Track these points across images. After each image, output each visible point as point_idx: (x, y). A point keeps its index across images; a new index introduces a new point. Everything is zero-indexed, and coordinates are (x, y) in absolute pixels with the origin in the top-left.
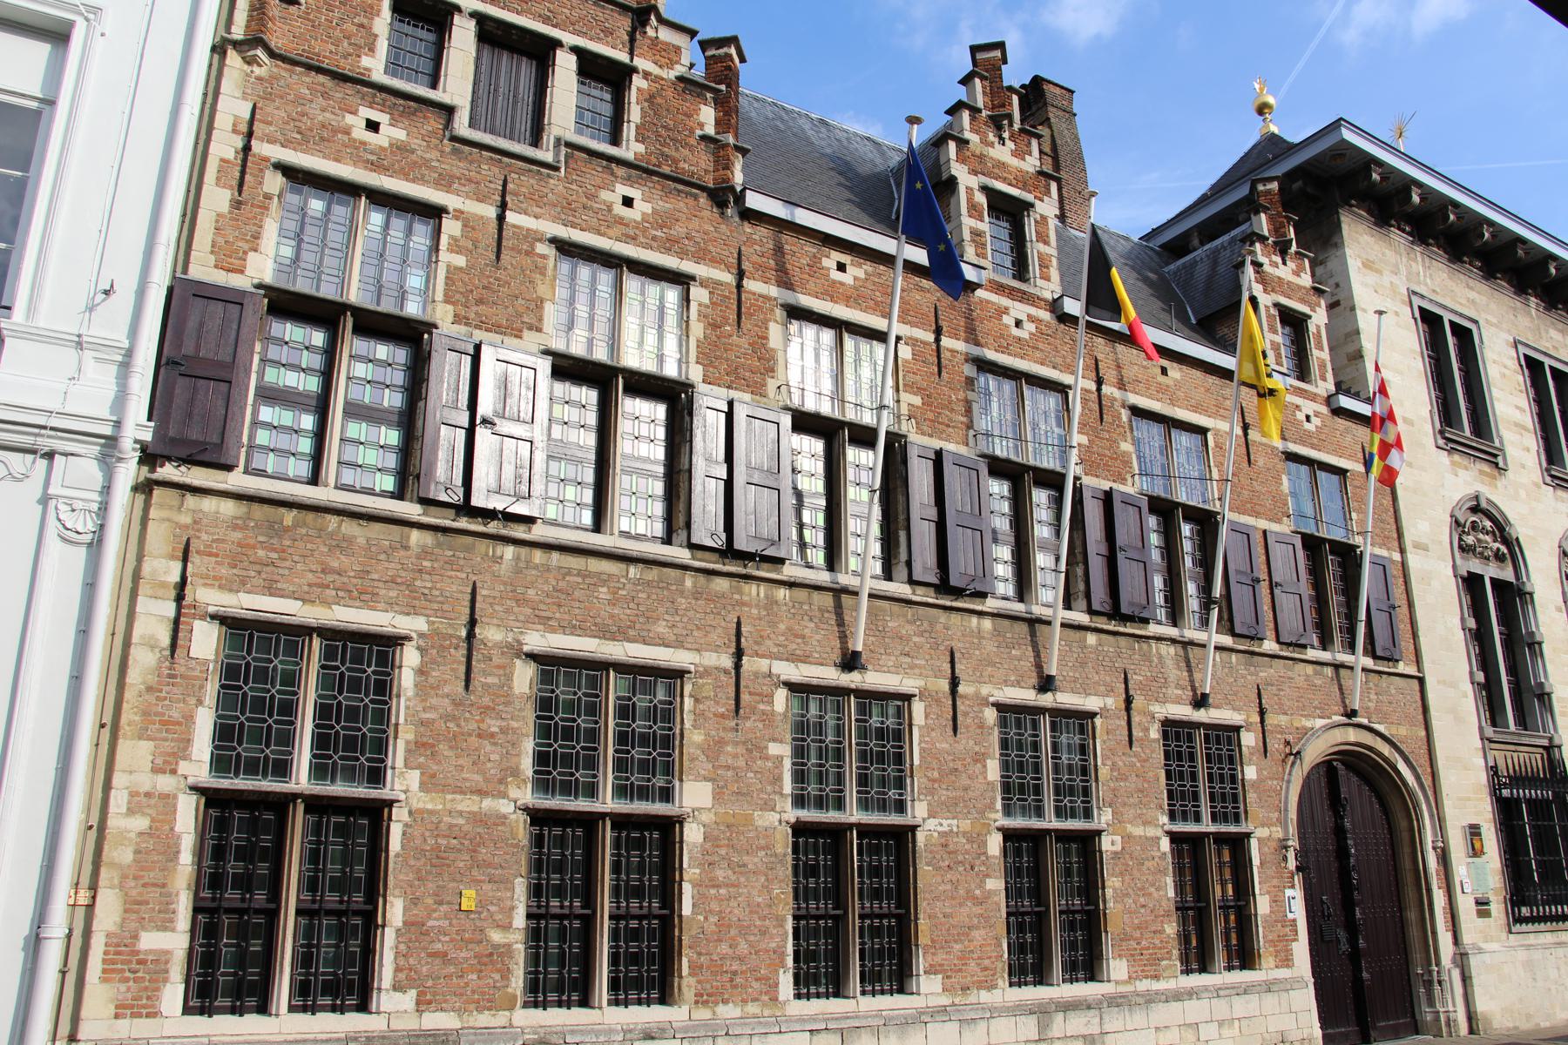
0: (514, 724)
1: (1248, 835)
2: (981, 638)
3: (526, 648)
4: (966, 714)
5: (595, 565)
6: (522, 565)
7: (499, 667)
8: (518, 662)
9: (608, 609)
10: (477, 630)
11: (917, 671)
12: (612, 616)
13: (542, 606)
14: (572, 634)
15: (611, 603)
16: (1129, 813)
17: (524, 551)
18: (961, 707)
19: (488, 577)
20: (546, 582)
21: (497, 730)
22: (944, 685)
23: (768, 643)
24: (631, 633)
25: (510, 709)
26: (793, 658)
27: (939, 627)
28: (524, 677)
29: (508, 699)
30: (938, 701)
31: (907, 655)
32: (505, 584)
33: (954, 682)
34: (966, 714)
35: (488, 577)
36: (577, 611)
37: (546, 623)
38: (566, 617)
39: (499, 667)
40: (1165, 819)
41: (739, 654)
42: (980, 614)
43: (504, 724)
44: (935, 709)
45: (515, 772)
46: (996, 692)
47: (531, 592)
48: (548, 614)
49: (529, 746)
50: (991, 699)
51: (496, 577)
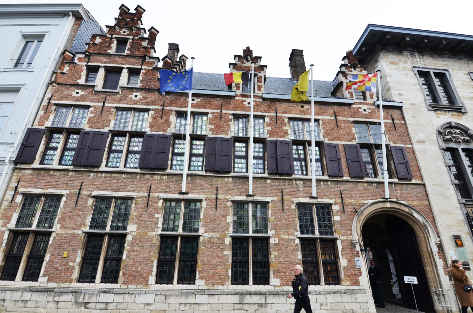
0: (86, 213)
5: (113, 175)
7: (85, 200)
8: (90, 198)
10: (81, 192)
11: (205, 193)
12: (116, 186)
13: (98, 185)
17: (96, 174)
19: (86, 180)
22: (214, 196)
23: (159, 189)
24: (121, 189)
26: (166, 192)
28: (91, 202)
29: (86, 206)
32: (90, 181)
34: (220, 204)
35: (86, 180)
37: (99, 189)
39: (85, 200)
43: (83, 212)
44: (210, 203)
48: (100, 187)
50: (230, 200)
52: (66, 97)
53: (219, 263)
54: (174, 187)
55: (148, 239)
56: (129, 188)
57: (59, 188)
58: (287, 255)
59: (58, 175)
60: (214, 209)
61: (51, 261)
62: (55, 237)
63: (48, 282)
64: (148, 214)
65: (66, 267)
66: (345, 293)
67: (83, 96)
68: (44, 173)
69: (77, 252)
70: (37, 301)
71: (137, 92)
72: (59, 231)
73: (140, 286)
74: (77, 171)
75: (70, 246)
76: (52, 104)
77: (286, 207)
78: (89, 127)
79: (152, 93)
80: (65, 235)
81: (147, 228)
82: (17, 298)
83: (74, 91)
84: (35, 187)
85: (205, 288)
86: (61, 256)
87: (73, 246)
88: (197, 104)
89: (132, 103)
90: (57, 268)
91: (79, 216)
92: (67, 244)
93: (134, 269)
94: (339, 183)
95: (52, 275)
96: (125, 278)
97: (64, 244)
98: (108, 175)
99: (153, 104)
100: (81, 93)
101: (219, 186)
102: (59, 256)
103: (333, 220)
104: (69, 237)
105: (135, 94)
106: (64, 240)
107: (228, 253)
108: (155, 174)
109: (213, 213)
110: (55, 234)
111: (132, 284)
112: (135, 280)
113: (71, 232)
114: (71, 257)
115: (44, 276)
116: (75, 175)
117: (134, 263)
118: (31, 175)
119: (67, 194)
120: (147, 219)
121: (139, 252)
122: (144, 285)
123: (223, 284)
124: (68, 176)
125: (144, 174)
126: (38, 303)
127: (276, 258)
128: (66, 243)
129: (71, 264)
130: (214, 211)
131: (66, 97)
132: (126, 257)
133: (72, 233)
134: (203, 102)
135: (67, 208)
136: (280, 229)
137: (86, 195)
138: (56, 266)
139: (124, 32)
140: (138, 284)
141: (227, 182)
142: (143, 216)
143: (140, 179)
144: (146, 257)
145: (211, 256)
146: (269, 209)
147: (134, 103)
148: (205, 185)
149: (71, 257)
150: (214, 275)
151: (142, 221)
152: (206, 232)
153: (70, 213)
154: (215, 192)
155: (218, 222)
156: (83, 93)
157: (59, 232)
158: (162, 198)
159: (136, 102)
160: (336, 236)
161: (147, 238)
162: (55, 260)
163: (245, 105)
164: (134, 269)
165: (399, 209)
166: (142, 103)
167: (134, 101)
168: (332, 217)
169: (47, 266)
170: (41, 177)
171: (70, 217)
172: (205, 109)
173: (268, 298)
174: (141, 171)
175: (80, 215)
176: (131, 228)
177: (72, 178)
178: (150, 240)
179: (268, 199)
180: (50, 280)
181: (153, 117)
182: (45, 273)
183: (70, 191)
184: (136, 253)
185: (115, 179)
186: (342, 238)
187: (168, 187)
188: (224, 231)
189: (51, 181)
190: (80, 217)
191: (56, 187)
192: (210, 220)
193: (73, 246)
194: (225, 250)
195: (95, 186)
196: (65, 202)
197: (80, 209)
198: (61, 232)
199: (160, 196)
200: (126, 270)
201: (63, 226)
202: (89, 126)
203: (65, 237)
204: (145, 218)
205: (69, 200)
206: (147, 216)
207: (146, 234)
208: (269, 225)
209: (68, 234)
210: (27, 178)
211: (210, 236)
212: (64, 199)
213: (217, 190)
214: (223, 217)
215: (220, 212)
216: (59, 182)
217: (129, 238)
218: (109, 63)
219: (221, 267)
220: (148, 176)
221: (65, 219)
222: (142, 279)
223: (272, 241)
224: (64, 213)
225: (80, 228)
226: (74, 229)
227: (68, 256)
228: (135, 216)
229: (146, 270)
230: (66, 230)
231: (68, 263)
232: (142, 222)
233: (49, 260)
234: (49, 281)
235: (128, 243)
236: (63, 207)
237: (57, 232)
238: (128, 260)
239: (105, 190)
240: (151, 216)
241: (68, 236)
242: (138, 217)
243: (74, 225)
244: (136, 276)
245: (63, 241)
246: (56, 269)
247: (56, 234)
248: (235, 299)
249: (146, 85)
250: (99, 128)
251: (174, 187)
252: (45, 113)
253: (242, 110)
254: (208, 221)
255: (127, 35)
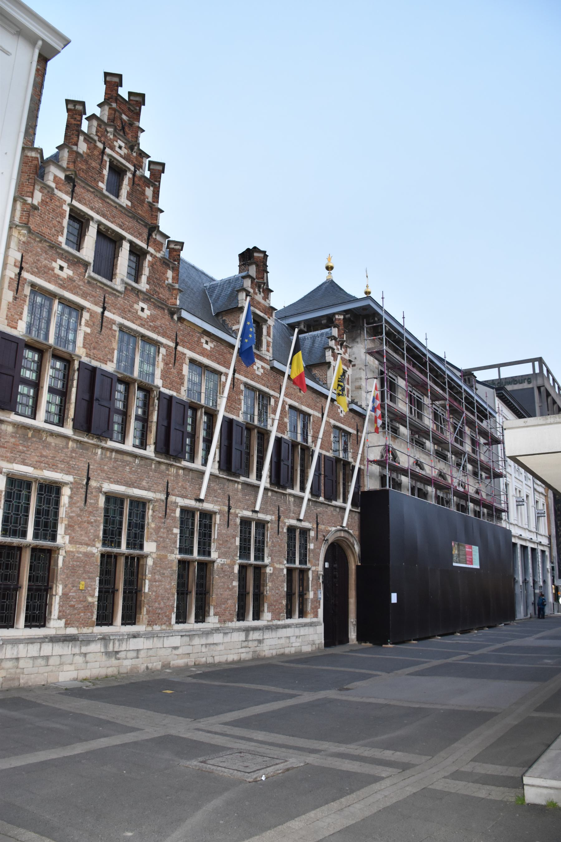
0: (99, 519)
1: (309, 569)
2: (238, 491)
3: (103, 490)
4: (231, 520)
6: (103, 457)
8: (100, 495)
9: (129, 475)
12: (130, 478)
13: (109, 473)
14: (117, 484)
15: (130, 472)
16: (276, 559)
17: (104, 452)
18: (230, 517)
20: (110, 464)
21: (92, 520)
22: (226, 509)
24: (135, 484)
25: (97, 513)
27: (226, 487)
28: (102, 500)
29: (97, 509)
30: (224, 515)
31: (215, 497)
32: (98, 464)
33: (229, 508)
35: (93, 461)
36: (119, 476)
37: (109, 479)
38: (116, 478)
40: (285, 562)
41: (168, 494)
42: (238, 483)
45: (98, 537)
46: (240, 512)
47: (106, 467)
48: (110, 476)
49: (102, 527)
50: (239, 515)
51: (95, 460)
52: (45, 272)
53: (229, 597)
54: (190, 489)
55: (168, 564)
56: (144, 483)
57: (59, 471)
58: (277, 587)
59: (53, 444)
60: (226, 527)
61: (65, 595)
62: (64, 557)
63: (66, 627)
64: (167, 528)
65: (84, 604)
66: (311, 626)
67: (70, 279)
68: (33, 436)
69: (95, 582)
70: (60, 656)
71: (144, 301)
72: (69, 548)
73: (164, 627)
74: (80, 442)
75: (85, 572)
76: (25, 279)
77: (280, 530)
78: (88, 355)
79: (162, 311)
80: (76, 555)
81: (166, 548)
82: (36, 654)
83: (56, 262)
84: (24, 463)
85: (218, 626)
86: (76, 587)
87: (89, 572)
88: (211, 351)
89: (138, 322)
90: (74, 606)
91: (89, 523)
92: (82, 569)
93: (157, 605)
94: (318, 504)
95: (69, 617)
96: (149, 617)
97: (77, 569)
98: (119, 457)
99: (164, 335)
100: (68, 272)
101: (231, 494)
102: (73, 586)
103: (308, 547)
104: (82, 558)
105: (142, 304)
106: (76, 561)
107: (236, 584)
108: (171, 465)
109: (225, 531)
110: (64, 551)
111: (156, 625)
112: (159, 619)
113: (83, 549)
114: (89, 589)
115: (59, 618)
116: (77, 447)
117: (157, 596)
118: (12, 437)
119: (71, 483)
120: (165, 536)
121: (160, 581)
122: (167, 626)
123: (232, 621)
124: (68, 448)
125: (159, 463)
126: (62, 657)
127: (271, 589)
128: (80, 567)
129: (90, 599)
130: (226, 529)
131: (45, 272)
132: (149, 588)
133: (85, 551)
134: (216, 350)
135: (74, 509)
136: (274, 556)
137: (95, 488)
138: (72, 603)
139: (120, 147)
140: (162, 624)
141: (237, 490)
142: (162, 530)
143: (155, 471)
144: (167, 589)
145: (223, 588)
146: (268, 531)
147: (141, 324)
148: (219, 491)
149: (89, 589)
150: (225, 610)
151: (161, 537)
152: (219, 557)
153: (79, 518)
154: (227, 502)
155: (229, 545)
156: (70, 273)
157: (69, 549)
158: (179, 504)
159: (143, 323)
160: (309, 565)
161: (167, 562)
162: (70, 594)
163: (255, 370)
164: (157, 605)
165: (347, 539)
166: (150, 326)
167: (140, 318)
168: (308, 544)
169: (61, 603)
170: (30, 444)
171: (80, 524)
172: (219, 363)
173: (265, 634)
174: (155, 457)
175: (92, 523)
176: (149, 547)
177: (74, 455)
178: (170, 565)
179: (268, 518)
180: (69, 624)
181: (164, 360)
182: (61, 614)
183: (75, 478)
184: (157, 583)
185: (128, 465)
186: (313, 568)
187: (184, 488)
188: (233, 557)
189: (45, 454)
190: (92, 526)
191: (53, 467)
192: (223, 541)
193: (89, 572)
194: (234, 580)
195: (105, 475)
196: (71, 497)
197: (91, 512)
198: (71, 550)
199: (177, 501)
200: (149, 607)
201: (73, 538)
202: (87, 353)
203: (78, 557)
204: (164, 533)
205: (75, 494)
206: (165, 531)
207: (166, 557)
208: (266, 551)
209: (81, 552)
210: (8, 442)
211: (223, 562)
212: (66, 492)
213: (229, 500)
214: (233, 538)
215: (231, 531)
216: (57, 459)
217: (150, 562)
218: (104, 216)
219: (231, 601)
220: (163, 467)
221: (74, 526)
222: (165, 618)
223: (269, 570)
224: (71, 518)
225: (94, 543)
226: (88, 545)
227: (86, 587)
228: (153, 529)
229: (169, 606)
230: (78, 546)
231: (86, 597)
232: (161, 539)
233: (63, 594)
234: (67, 625)
235: (149, 568)
236: (69, 506)
237: (68, 549)
238: (150, 593)
239: (117, 482)
240: (170, 530)
241: (81, 555)
242: (157, 530)
243: (87, 539)
244: (159, 614)
245: (75, 563)
246: (73, 606)
247: (65, 552)
248: (242, 636)
249: (155, 290)
250: (99, 360)
251: (190, 489)
252: (15, 298)
253: (252, 379)
254: (221, 542)
255: (124, 158)
